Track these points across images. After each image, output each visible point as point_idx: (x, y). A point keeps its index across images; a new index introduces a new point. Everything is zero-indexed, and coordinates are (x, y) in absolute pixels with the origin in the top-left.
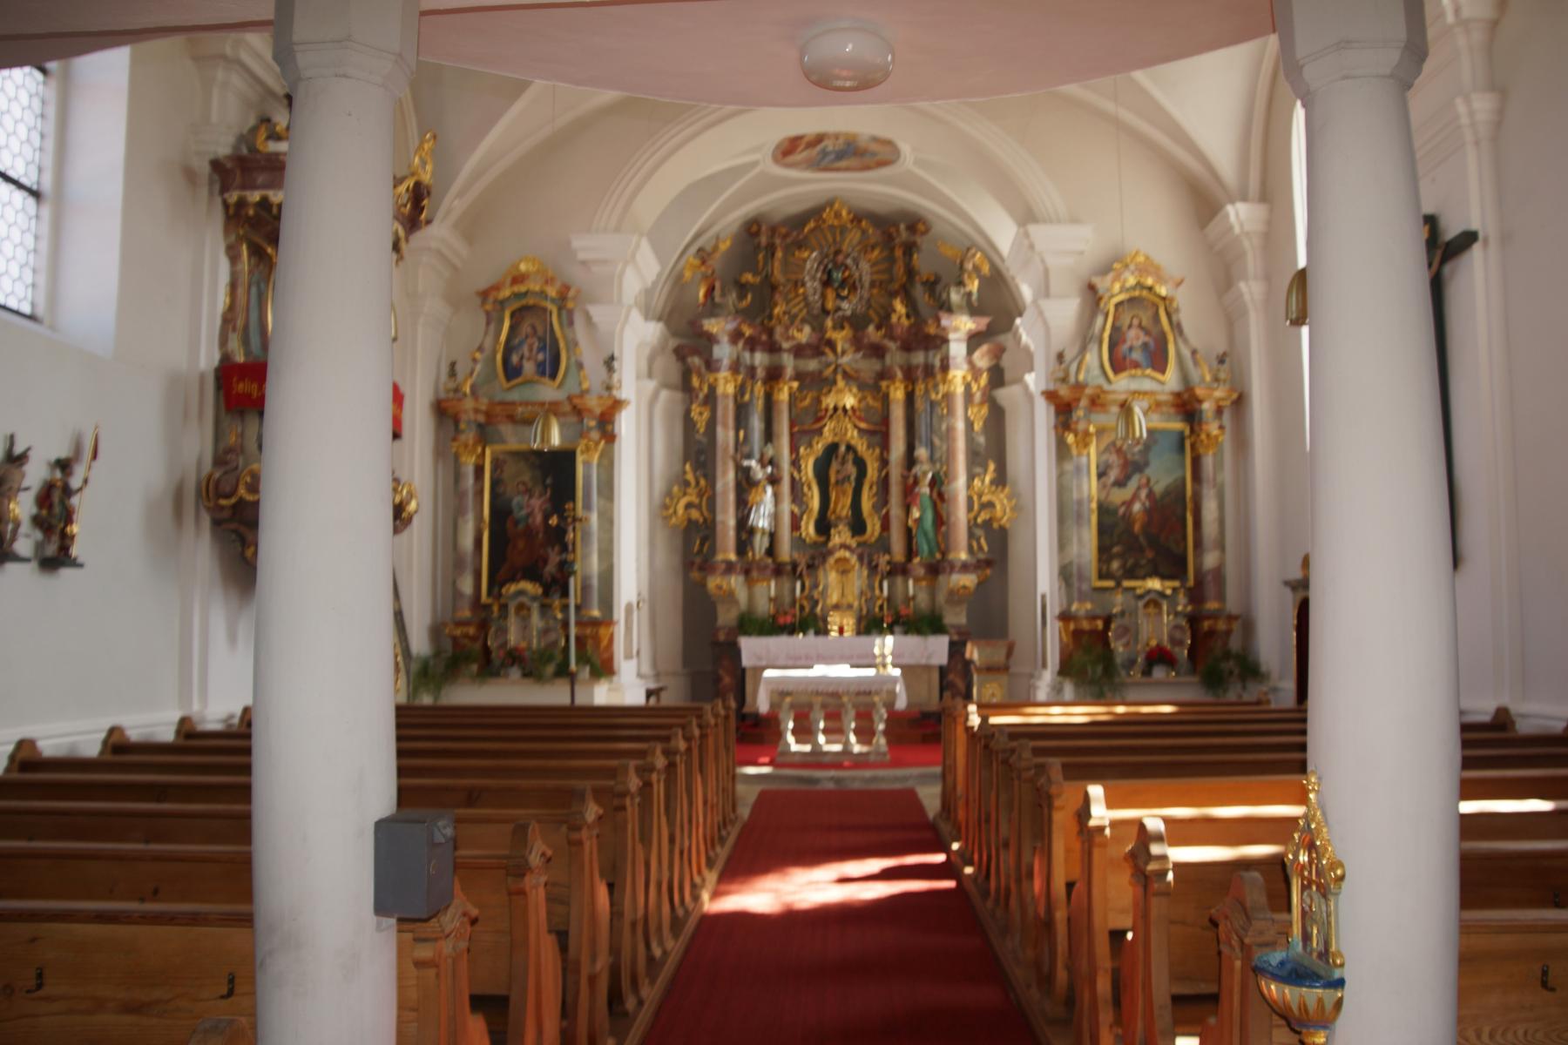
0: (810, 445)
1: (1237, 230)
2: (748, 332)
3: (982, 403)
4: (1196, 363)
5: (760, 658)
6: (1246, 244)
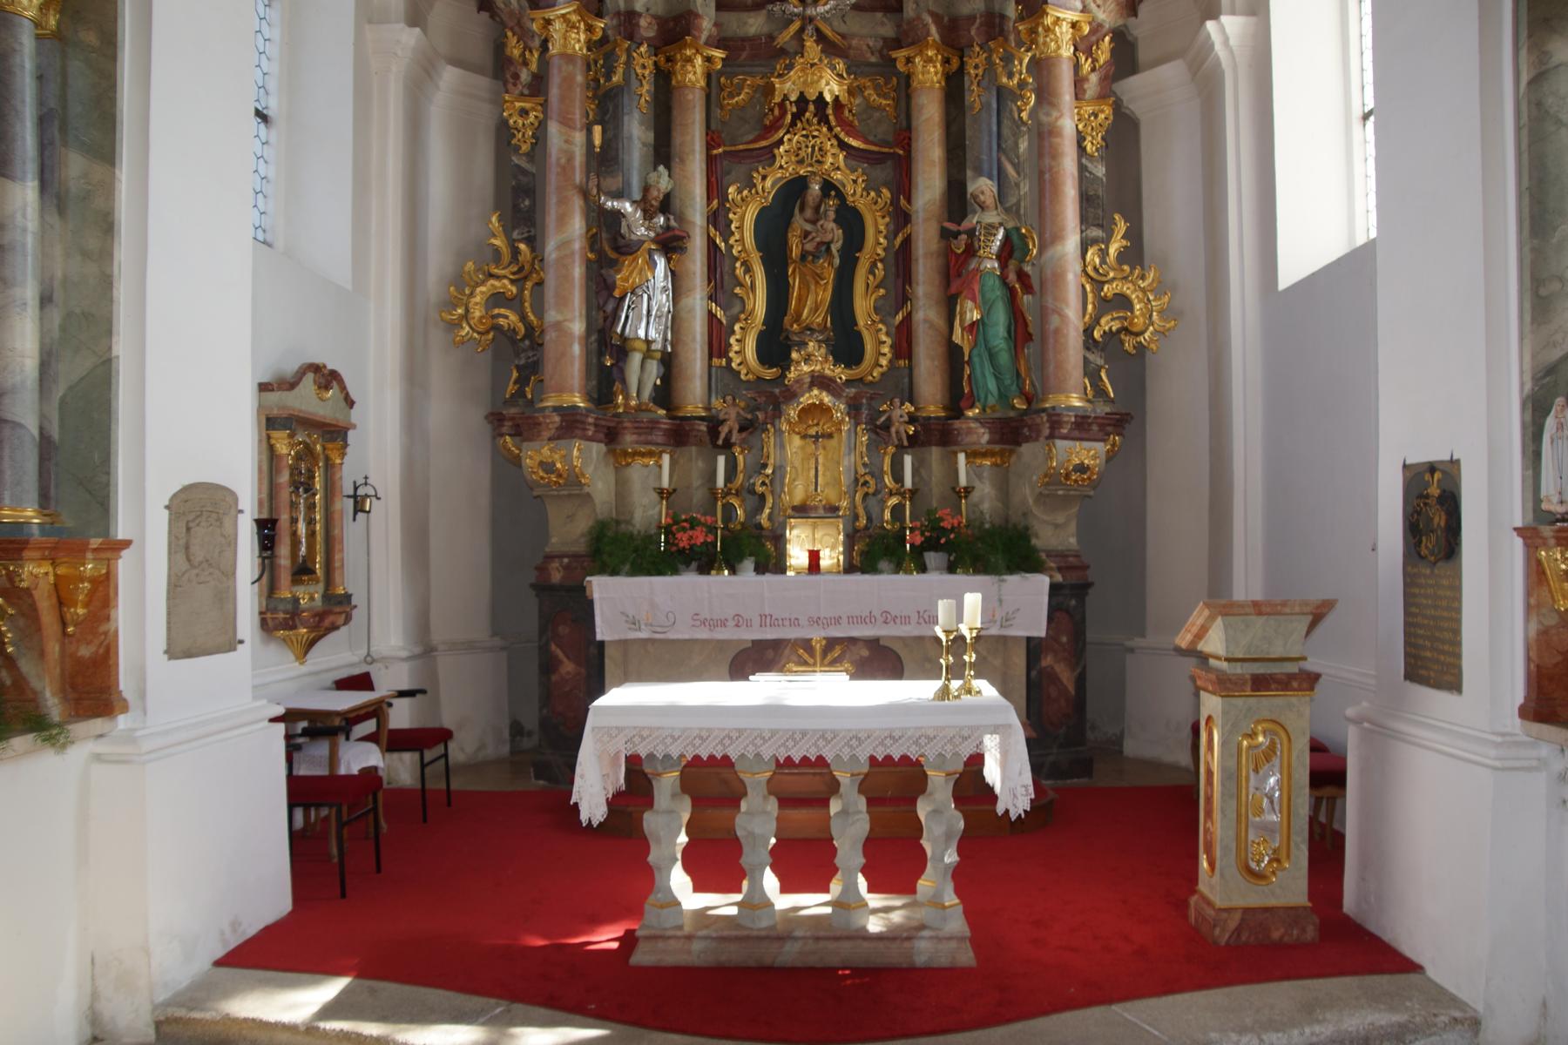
0: (751, 185)
5: (634, 623)
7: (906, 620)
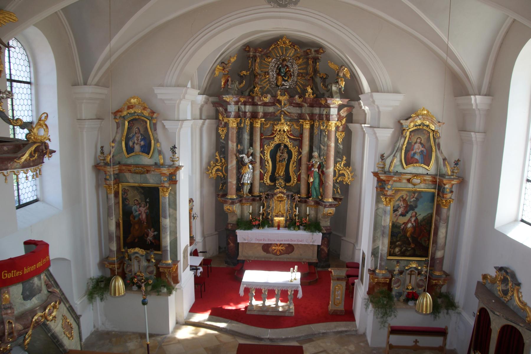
1: (474, 107)
2: (242, 100)
3: (342, 131)
4: (445, 165)
5: (245, 240)
6: (477, 112)
7: (295, 241)
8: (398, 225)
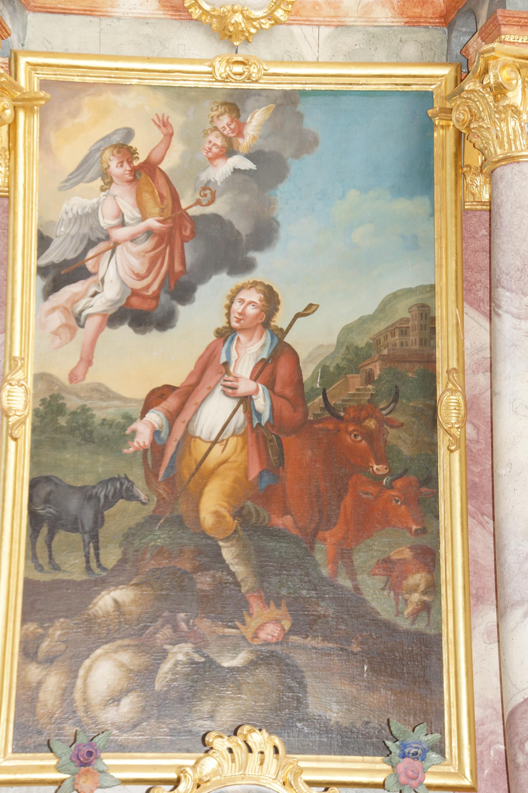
8: (103, 412)
